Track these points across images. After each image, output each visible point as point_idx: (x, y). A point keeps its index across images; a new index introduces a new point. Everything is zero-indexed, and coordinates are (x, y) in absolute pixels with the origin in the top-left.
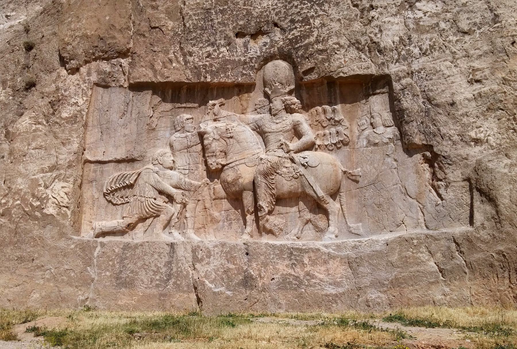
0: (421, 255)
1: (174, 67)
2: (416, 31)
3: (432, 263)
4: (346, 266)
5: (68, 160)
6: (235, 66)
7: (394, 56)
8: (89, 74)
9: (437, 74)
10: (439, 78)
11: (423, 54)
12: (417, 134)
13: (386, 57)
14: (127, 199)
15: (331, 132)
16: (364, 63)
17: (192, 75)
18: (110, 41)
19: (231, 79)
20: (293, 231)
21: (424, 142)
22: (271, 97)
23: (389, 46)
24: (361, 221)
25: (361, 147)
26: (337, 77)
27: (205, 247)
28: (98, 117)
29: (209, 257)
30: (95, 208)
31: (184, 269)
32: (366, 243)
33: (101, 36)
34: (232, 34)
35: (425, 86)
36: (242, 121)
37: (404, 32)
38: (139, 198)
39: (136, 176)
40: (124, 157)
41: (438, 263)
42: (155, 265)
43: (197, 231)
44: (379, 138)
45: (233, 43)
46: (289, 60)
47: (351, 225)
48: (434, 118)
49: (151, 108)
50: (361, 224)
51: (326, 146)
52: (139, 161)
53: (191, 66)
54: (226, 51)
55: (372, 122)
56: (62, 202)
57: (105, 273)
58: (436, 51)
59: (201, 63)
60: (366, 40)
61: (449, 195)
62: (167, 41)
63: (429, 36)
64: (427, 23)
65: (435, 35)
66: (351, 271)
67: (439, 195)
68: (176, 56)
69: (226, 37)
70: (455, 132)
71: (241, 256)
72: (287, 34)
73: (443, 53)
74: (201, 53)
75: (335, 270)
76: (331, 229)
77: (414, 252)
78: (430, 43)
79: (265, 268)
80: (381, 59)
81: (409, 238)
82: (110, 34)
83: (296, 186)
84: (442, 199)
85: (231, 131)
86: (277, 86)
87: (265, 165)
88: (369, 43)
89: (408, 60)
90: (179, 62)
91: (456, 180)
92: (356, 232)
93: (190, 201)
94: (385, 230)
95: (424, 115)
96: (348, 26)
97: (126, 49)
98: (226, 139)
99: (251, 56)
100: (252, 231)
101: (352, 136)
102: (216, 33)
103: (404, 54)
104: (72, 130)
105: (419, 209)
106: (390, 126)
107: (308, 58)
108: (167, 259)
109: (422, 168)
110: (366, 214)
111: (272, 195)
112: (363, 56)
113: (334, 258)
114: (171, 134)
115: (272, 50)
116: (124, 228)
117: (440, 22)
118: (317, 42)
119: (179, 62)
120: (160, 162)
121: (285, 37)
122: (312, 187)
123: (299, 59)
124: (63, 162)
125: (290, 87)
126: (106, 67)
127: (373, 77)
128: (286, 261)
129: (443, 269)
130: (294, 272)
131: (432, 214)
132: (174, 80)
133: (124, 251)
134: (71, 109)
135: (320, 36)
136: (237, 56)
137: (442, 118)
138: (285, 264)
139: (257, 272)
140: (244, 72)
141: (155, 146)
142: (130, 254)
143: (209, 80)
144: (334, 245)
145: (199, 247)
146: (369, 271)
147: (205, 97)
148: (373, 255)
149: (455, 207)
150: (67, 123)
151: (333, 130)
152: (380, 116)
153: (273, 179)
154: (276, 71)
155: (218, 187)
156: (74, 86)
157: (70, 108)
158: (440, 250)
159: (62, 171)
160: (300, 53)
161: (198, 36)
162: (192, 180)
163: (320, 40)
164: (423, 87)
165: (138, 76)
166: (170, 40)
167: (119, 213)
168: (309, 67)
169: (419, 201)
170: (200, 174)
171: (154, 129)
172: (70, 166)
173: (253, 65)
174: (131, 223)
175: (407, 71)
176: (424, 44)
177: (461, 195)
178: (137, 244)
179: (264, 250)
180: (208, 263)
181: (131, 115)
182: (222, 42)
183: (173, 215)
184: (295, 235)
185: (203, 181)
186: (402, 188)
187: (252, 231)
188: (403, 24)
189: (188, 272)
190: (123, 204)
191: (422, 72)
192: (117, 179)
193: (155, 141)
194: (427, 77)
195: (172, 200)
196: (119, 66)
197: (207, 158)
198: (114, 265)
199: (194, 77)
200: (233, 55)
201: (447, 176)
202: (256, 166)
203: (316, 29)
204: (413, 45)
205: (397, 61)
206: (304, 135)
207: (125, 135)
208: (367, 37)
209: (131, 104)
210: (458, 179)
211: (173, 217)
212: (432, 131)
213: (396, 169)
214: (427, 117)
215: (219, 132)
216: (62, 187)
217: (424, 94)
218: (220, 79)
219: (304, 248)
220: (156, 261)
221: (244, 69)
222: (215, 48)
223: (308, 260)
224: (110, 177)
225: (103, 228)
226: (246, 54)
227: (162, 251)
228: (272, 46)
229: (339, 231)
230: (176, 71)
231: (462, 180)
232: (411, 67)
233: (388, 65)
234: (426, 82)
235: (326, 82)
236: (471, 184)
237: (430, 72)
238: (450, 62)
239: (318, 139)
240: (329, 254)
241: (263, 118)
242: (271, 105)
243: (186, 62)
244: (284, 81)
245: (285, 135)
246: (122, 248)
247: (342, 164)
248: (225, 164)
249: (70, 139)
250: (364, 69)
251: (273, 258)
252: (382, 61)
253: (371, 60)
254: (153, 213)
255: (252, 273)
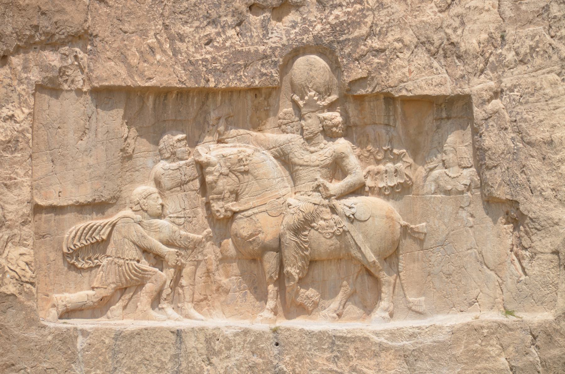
0: (490, 349)
1: (158, 62)
2: (514, 21)
3: (503, 359)
4: (401, 361)
5: (21, 213)
6: (250, 61)
7: (478, 65)
8: (26, 69)
9: (536, 94)
10: (538, 101)
11: (521, 61)
12: (500, 185)
13: (467, 67)
14: (96, 261)
15: (387, 169)
16: (436, 76)
17: (186, 75)
18: (57, 17)
19: (244, 82)
20: (332, 306)
21: (509, 197)
22: (304, 111)
23: (472, 51)
24: (424, 295)
25: (427, 193)
26: (397, 96)
27: (223, 336)
28: (46, 137)
29: (229, 349)
30: (51, 274)
31: (197, 363)
32: (427, 330)
33: (44, 8)
34: (243, 6)
35: (518, 113)
36: (261, 144)
37: (496, 25)
38: (116, 260)
39: (110, 229)
40: (90, 200)
41: (509, 359)
42: (158, 359)
43: (197, 304)
44: (452, 183)
45: (245, 21)
46: (330, 56)
47: (411, 299)
48: (524, 163)
49: (125, 124)
50: (423, 298)
51: (380, 189)
52: (112, 205)
53: (184, 60)
54: (236, 36)
55: (444, 159)
56: (24, 276)
57: (94, 371)
58: (539, 57)
59: (198, 57)
60: (441, 39)
61: (534, 269)
62: (143, 15)
63: (530, 29)
64: (533, 6)
65: (540, 29)
66: (406, 366)
67: (523, 269)
68: (159, 41)
69: (236, 12)
70: (548, 185)
71: (269, 347)
72: (327, 12)
73: (548, 61)
74: (197, 38)
75: (387, 365)
76: (384, 304)
77: (483, 344)
78: (531, 43)
79: (300, 361)
80: (460, 69)
81: (478, 326)
82: (56, 5)
83: (338, 245)
84: (526, 274)
85: (245, 163)
86: (311, 96)
87: (296, 216)
88: (444, 43)
89: (498, 70)
90: (164, 51)
91: (543, 251)
92: (417, 309)
93: (187, 263)
94: (454, 308)
95: (511, 158)
96: (417, 11)
97: (83, 31)
98: (238, 174)
99: (274, 45)
100: (276, 307)
101: (417, 177)
102: (220, 4)
103: (493, 61)
104: (16, 163)
105: (497, 284)
106: (468, 167)
107: (358, 60)
108: (173, 351)
109: (505, 230)
110: (431, 285)
111: (303, 258)
112: (436, 64)
113: (386, 349)
114: (156, 162)
115: (305, 37)
116: (96, 304)
117: (552, 3)
118: (371, 34)
119: (164, 51)
120: (143, 207)
121: (323, 17)
122: (360, 249)
123: (344, 60)
124: (13, 216)
125: (330, 98)
126: (53, 58)
127: (448, 98)
128: (326, 353)
129: (514, 366)
130: (337, 366)
131: (512, 293)
132: (161, 84)
133: (116, 341)
134: (5, 127)
135: (377, 25)
136: (252, 45)
137: (535, 164)
138: (325, 356)
139: (291, 368)
140: (264, 71)
141: (132, 181)
142: (124, 345)
143: (212, 85)
144: (386, 333)
145: (214, 335)
146: (428, 367)
147: (203, 104)
148: (434, 347)
149: (539, 286)
150: (4, 150)
151: (390, 166)
152: (454, 152)
153: (306, 235)
154: (311, 73)
155: (228, 243)
156: (4, 87)
157: (4, 124)
158: (513, 343)
159: (16, 231)
160: (347, 50)
161: (192, 8)
162: (189, 232)
163: (376, 31)
164: (514, 113)
165: (105, 75)
166: (148, 12)
167: (86, 280)
168: (359, 76)
169: (499, 274)
170: (201, 222)
171: (130, 157)
172: (24, 223)
173: (276, 59)
174: (106, 297)
175: (495, 89)
176: (522, 45)
177: (548, 271)
178: (132, 332)
179: (299, 338)
180: (228, 357)
181: (96, 135)
182: (230, 20)
183: (165, 282)
184: (335, 311)
185: (205, 233)
186: (478, 255)
187: (276, 305)
188: (496, 10)
189: (202, 368)
190: (91, 268)
191: (516, 90)
192: (82, 234)
193: (132, 173)
194: (521, 99)
195: (162, 261)
196: (72, 56)
197: (211, 201)
198: (105, 362)
199: (189, 79)
200: (246, 43)
201: (533, 245)
202: (283, 215)
203: (370, 12)
204: (507, 47)
205: (482, 72)
206: (350, 174)
207: (89, 167)
208: (442, 34)
209: (95, 118)
210: (547, 250)
211: (166, 287)
212: (519, 182)
213: (473, 229)
214: (515, 162)
215: (228, 164)
216: (21, 255)
217: (514, 126)
218: (228, 83)
219: (349, 335)
220: (159, 354)
221: (263, 65)
222: (219, 29)
223: (354, 352)
224: (70, 230)
225: (68, 305)
226: (265, 41)
227: (166, 340)
228: (305, 31)
229: (394, 307)
230: (161, 68)
231: (551, 252)
232: (501, 82)
233: (469, 80)
234: (520, 107)
235: (382, 96)
236: (559, 259)
237: (527, 90)
238: (556, 73)
239: (369, 178)
240: (380, 344)
241: (290, 142)
242: (303, 123)
243: (176, 52)
244: (322, 90)
245: (324, 171)
246: (113, 338)
247: (401, 215)
248: (238, 210)
249: (15, 179)
250: (436, 86)
251: (310, 349)
252: (461, 73)
253: (446, 71)
254: (136, 280)
255: (285, 369)
